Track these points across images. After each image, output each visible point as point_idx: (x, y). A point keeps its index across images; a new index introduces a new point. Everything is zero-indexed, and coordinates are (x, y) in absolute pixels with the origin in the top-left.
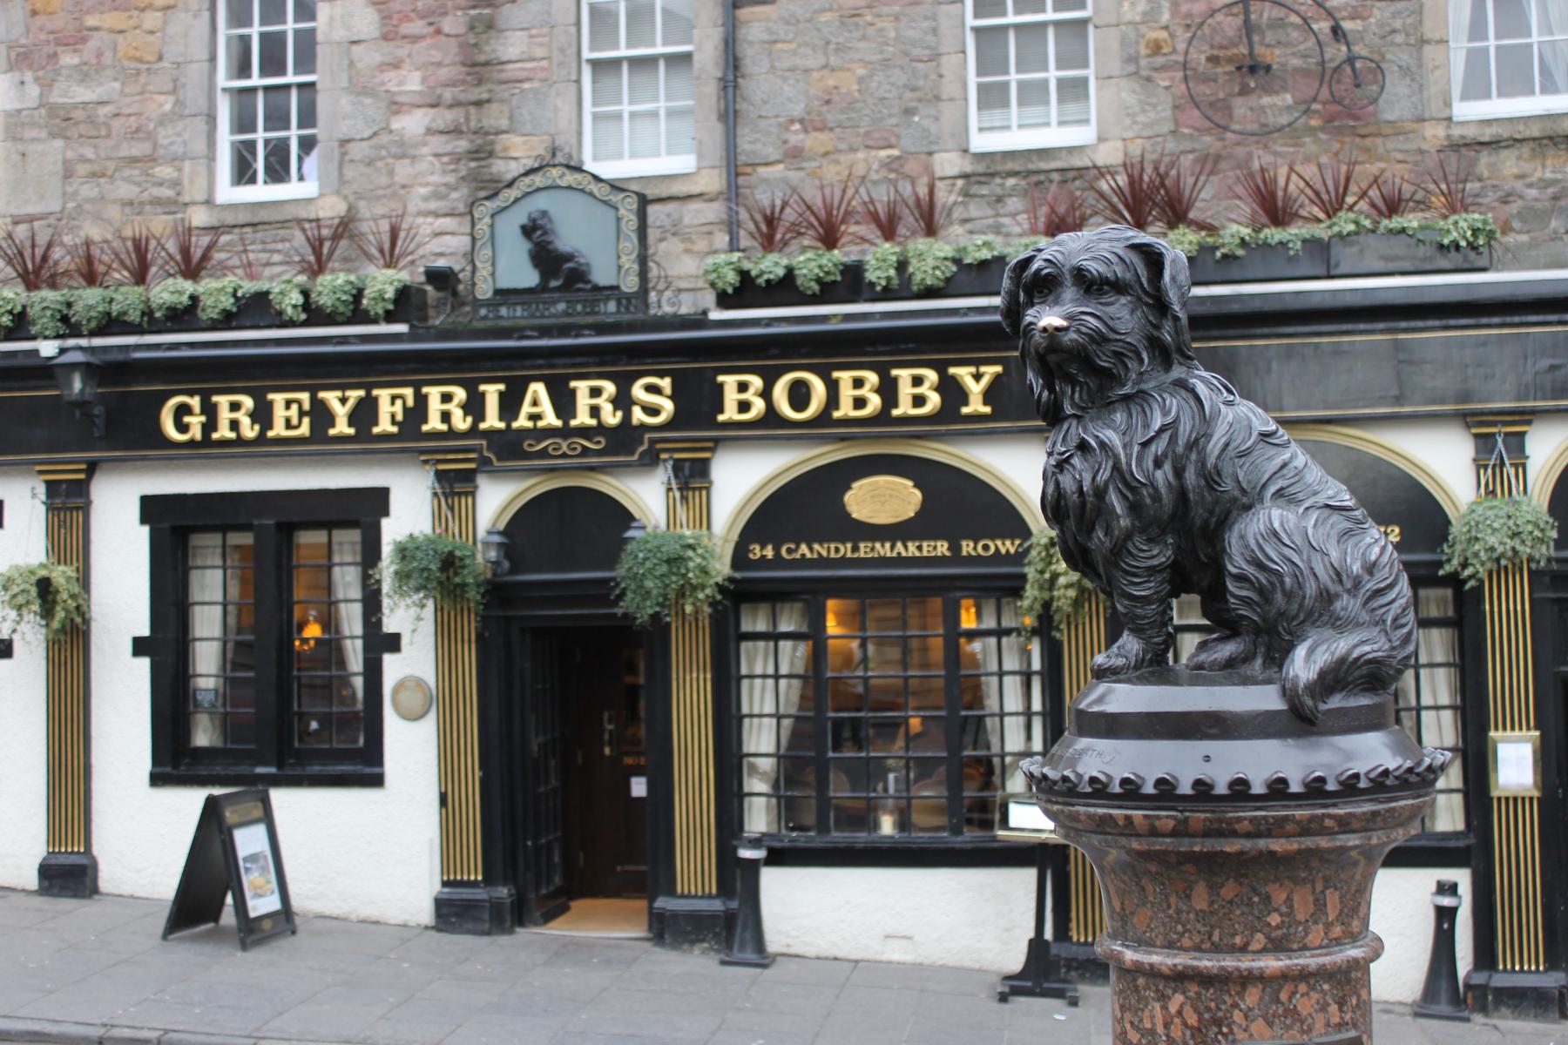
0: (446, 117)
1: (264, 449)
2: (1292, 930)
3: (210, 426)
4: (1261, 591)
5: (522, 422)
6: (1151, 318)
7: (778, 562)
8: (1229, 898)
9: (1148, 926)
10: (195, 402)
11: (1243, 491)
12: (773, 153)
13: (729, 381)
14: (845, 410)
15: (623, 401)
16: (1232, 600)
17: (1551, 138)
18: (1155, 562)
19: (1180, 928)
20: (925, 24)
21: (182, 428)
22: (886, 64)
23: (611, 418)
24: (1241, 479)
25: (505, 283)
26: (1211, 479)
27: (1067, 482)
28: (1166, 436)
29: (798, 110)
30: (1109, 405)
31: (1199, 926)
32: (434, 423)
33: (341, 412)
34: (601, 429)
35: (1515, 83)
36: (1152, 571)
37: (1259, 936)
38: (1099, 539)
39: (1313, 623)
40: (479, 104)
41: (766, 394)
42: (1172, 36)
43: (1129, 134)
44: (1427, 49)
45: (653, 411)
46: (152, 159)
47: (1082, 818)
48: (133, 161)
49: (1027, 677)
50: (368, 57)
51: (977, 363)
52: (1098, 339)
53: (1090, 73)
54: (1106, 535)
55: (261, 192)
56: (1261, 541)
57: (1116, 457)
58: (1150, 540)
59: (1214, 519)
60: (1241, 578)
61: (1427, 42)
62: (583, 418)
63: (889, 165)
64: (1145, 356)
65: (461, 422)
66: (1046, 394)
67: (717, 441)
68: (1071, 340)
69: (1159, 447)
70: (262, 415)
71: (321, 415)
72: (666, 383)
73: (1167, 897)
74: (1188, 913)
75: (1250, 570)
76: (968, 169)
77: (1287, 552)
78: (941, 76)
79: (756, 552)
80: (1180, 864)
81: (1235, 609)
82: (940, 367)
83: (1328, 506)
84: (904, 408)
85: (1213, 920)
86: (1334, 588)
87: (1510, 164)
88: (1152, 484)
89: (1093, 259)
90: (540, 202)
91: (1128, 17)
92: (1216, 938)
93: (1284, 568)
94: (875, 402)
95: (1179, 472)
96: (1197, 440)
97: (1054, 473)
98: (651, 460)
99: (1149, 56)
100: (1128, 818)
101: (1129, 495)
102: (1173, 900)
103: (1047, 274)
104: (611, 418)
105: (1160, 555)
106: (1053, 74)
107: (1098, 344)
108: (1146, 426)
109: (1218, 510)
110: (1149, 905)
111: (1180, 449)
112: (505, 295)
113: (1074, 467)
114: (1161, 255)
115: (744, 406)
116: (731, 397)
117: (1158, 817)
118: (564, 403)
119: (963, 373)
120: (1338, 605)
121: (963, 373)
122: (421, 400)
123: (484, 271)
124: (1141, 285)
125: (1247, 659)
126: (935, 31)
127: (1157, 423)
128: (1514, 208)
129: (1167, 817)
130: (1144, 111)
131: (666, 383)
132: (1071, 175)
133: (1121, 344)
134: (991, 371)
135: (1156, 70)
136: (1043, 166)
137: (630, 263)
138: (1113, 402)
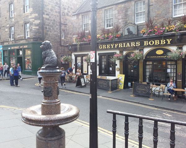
0: (123, 20)
1: (107, 49)
3: (103, 48)
5: (127, 46)
10: (102, 46)
13: (145, 42)
14: (156, 44)
15: (135, 44)
20: (168, 5)
21: (101, 48)
22: (164, 10)
23: (134, 46)
25: (125, 34)
29: (155, 15)
32: (120, 47)
33: (112, 46)
34: (133, 47)
40: (126, 18)
41: (148, 43)
45: (138, 45)
46: (100, 26)
48: (99, 26)
49: (174, 69)
50: (117, 15)
55: (109, 28)
62: (132, 46)
63: (164, 20)
65: (122, 47)
70: (106, 47)
71: (111, 46)
72: (139, 42)
90: (128, 27)
94: (159, 43)
98: (138, 49)
104: (134, 46)
112: (125, 35)
115: (146, 44)
116: (145, 43)
118: (130, 45)
119: (168, 40)
121: (168, 40)
122: (119, 45)
123: (124, 33)
126: (169, 6)
131: (139, 42)
134: (170, 40)
137: (136, 32)
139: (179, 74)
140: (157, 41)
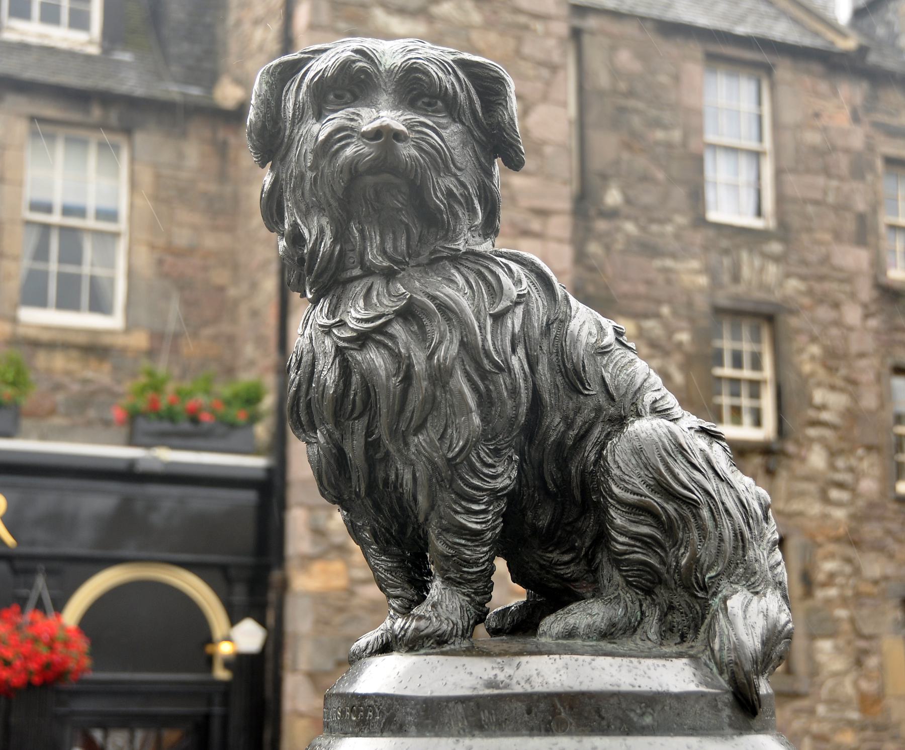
4: (667, 527)
6: (483, 160)
11: (611, 397)
16: (622, 539)
18: (500, 483)
24: (608, 380)
28: (520, 310)
30: (433, 263)
35: (68, 302)
36: (494, 494)
39: (729, 577)
56: (669, 460)
57: (463, 324)
58: (496, 452)
59: (572, 433)
60: (639, 510)
66: (328, 240)
68: (410, 156)
69: (515, 321)
75: (655, 500)
77: (698, 476)
81: (625, 553)
86: (745, 529)
87: (59, 362)
88: (510, 370)
93: (698, 496)
95: (532, 363)
96: (548, 325)
97: (339, 351)
101: (476, 378)
103: (362, 70)
109: (579, 421)
113: (392, 337)
114: (500, 81)
120: (751, 553)
124: (474, 112)
125: (631, 629)
128: (60, 397)
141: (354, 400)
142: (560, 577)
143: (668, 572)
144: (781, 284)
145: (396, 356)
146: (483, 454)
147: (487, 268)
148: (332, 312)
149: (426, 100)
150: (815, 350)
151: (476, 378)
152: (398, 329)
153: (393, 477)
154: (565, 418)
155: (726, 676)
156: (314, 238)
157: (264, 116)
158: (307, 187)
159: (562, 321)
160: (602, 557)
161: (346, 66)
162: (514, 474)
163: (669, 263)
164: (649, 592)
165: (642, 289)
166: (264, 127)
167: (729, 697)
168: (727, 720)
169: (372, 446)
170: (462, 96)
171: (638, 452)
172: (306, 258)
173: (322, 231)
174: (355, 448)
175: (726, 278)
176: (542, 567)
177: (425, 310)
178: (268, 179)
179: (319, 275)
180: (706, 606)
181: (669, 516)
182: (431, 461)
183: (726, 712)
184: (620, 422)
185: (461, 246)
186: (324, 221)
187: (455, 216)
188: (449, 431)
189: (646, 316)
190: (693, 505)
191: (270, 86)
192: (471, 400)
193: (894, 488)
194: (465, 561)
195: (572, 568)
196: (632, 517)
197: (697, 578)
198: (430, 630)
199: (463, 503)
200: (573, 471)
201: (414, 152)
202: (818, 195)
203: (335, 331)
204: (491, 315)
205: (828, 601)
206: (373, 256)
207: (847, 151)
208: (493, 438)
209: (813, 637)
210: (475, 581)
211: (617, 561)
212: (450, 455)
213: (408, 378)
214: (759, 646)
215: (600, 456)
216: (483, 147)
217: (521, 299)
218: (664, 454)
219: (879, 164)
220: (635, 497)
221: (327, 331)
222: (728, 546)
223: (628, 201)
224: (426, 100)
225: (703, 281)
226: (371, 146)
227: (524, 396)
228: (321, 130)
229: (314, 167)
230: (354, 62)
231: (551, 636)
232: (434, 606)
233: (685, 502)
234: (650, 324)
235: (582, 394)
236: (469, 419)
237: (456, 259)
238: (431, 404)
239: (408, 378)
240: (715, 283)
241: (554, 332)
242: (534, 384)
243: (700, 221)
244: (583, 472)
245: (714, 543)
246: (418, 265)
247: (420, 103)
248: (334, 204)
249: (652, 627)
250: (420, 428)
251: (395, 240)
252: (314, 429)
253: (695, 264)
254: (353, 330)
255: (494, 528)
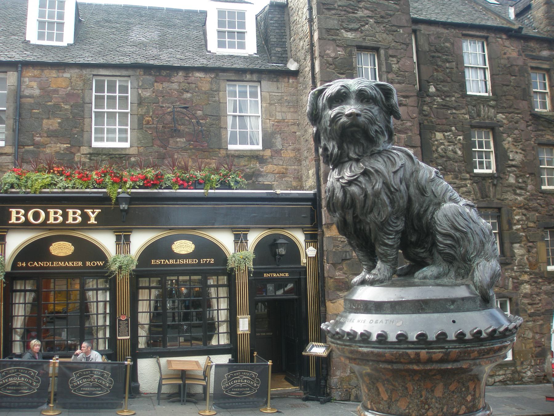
2: (474, 403)
4: (457, 241)
7: (27, 267)
8: (453, 390)
9: (408, 406)
11: (436, 196)
12: (29, 142)
13: (14, 211)
14: (51, 221)
16: (442, 246)
17: (253, 156)
19: (427, 407)
24: (434, 190)
26: (422, 191)
27: (354, 189)
30: (372, 155)
31: (437, 405)
36: (397, 232)
37: (463, 407)
38: (375, 216)
39: (478, 256)
41: (26, 215)
42: (153, 119)
43: (140, 146)
44: (222, 129)
47: (386, 355)
51: (93, 208)
52: (372, 121)
53: (129, 128)
54: (379, 214)
56: (456, 217)
57: (384, 176)
58: (397, 218)
59: (422, 209)
60: (447, 236)
61: (222, 128)
64: (386, 133)
66: (336, 150)
67: (8, 229)
68: (362, 121)
69: (400, 174)
73: (420, 392)
74: (432, 399)
75: (452, 232)
76: (91, 152)
77: (466, 223)
78: (84, 124)
79: (20, 264)
80: (435, 375)
81: (442, 250)
82: (82, 209)
83: (468, 205)
84: (70, 221)
85: (444, 401)
86: (484, 239)
89: (365, 86)
91: (141, 113)
92: (445, 410)
94: (61, 219)
95: (408, 187)
96: (412, 173)
97: (342, 187)
99: (146, 124)
100: (418, 354)
101: (389, 194)
102: (424, 393)
103: (344, 92)
105: (400, 225)
106: (117, 127)
107: (372, 124)
108: (394, 164)
109: (424, 205)
110: (409, 396)
111: (408, 176)
113: (360, 182)
114: (390, 90)
115: (18, 219)
117: (434, 353)
119: (89, 211)
120: (486, 247)
121: (89, 211)
124: (383, 101)
127: (399, 163)
129: (439, 352)
130: (144, 139)
132: (122, 156)
133: (377, 126)
134: (97, 211)
135: (147, 128)
136: (114, 153)
138: (374, 154)
139: (123, 318)
140: (56, 213)
141: (348, 203)
142: (420, 257)
143: (457, 255)
144: (495, 117)
145: (362, 188)
146: (393, 220)
147: (390, 155)
148: (339, 173)
149: (366, 100)
150: (510, 139)
151: (389, 194)
152: (361, 179)
153: (362, 228)
154: (420, 204)
155: (478, 291)
156: (331, 149)
157: (312, 109)
158: (328, 132)
159: (417, 171)
160: (434, 251)
161: (339, 91)
162: (403, 225)
163: (454, 111)
164: (451, 263)
165: (444, 121)
166: (312, 113)
167: (480, 298)
168: (479, 305)
169: (355, 217)
170: (378, 97)
171: (445, 216)
172: (329, 155)
173: (334, 146)
174: (349, 218)
175: (475, 116)
176: (414, 254)
177: (370, 171)
178: (315, 129)
179: (334, 161)
180: (471, 266)
181: (457, 237)
182: (375, 222)
183: (479, 303)
184: (439, 205)
185: (381, 148)
186: (335, 143)
187: (379, 138)
188: (381, 213)
189: (446, 132)
190: (465, 233)
191: (314, 98)
192: (387, 201)
193: (541, 188)
194: (389, 255)
195: (425, 254)
196: (444, 238)
197: (467, 257)
198: (377, 278)
199: (387, 236)
200: (424, 222)
201: (364, 119)
202: (508, 83)
203: (341, 180)
204: (393, 172)
205: (517, 230)
206: (352, 155)
207: (517, 66)
208: (396, 214)
209: (512, 243)
210: (392, 261)
211: (440, 252)
212: (382, 220)
213: (366, 196)
214: (488, 279)
215: (432, 217)
216: (387, 113)
217: (403, 166)
218: (455, 216)
219: (529, 69)
220: (445, 231)
221: (338, 180)
222: (478, 246)
223: (437, 90)
224: (366, 100)
225: (467, 116)
226: (349, 119)
227: (406, 198)
228: (332, 113)
229: (330, 125)
230: (341, 90)
231: (418, 279)
232: (379, 270)
233: (462, 232)
234: (448, 133)
235: (425, 196)
236: (387, 209)
237: (380, 153)
238: (374, 203)
239: (366, 196)
240: (472, 117)
241: (414, 175)
242: (409, 194)
243: (464, 95)
244: (427, 222)
245: (473, 245)
246: (367, 156)
247: (364, 101)
248: (338, 138)
249: (452, 274)
250: (371, 211)
251: (359, 149)
252: (335, 212)
253: (463, 111)
254: (347, 180)
255: (398, 243)
